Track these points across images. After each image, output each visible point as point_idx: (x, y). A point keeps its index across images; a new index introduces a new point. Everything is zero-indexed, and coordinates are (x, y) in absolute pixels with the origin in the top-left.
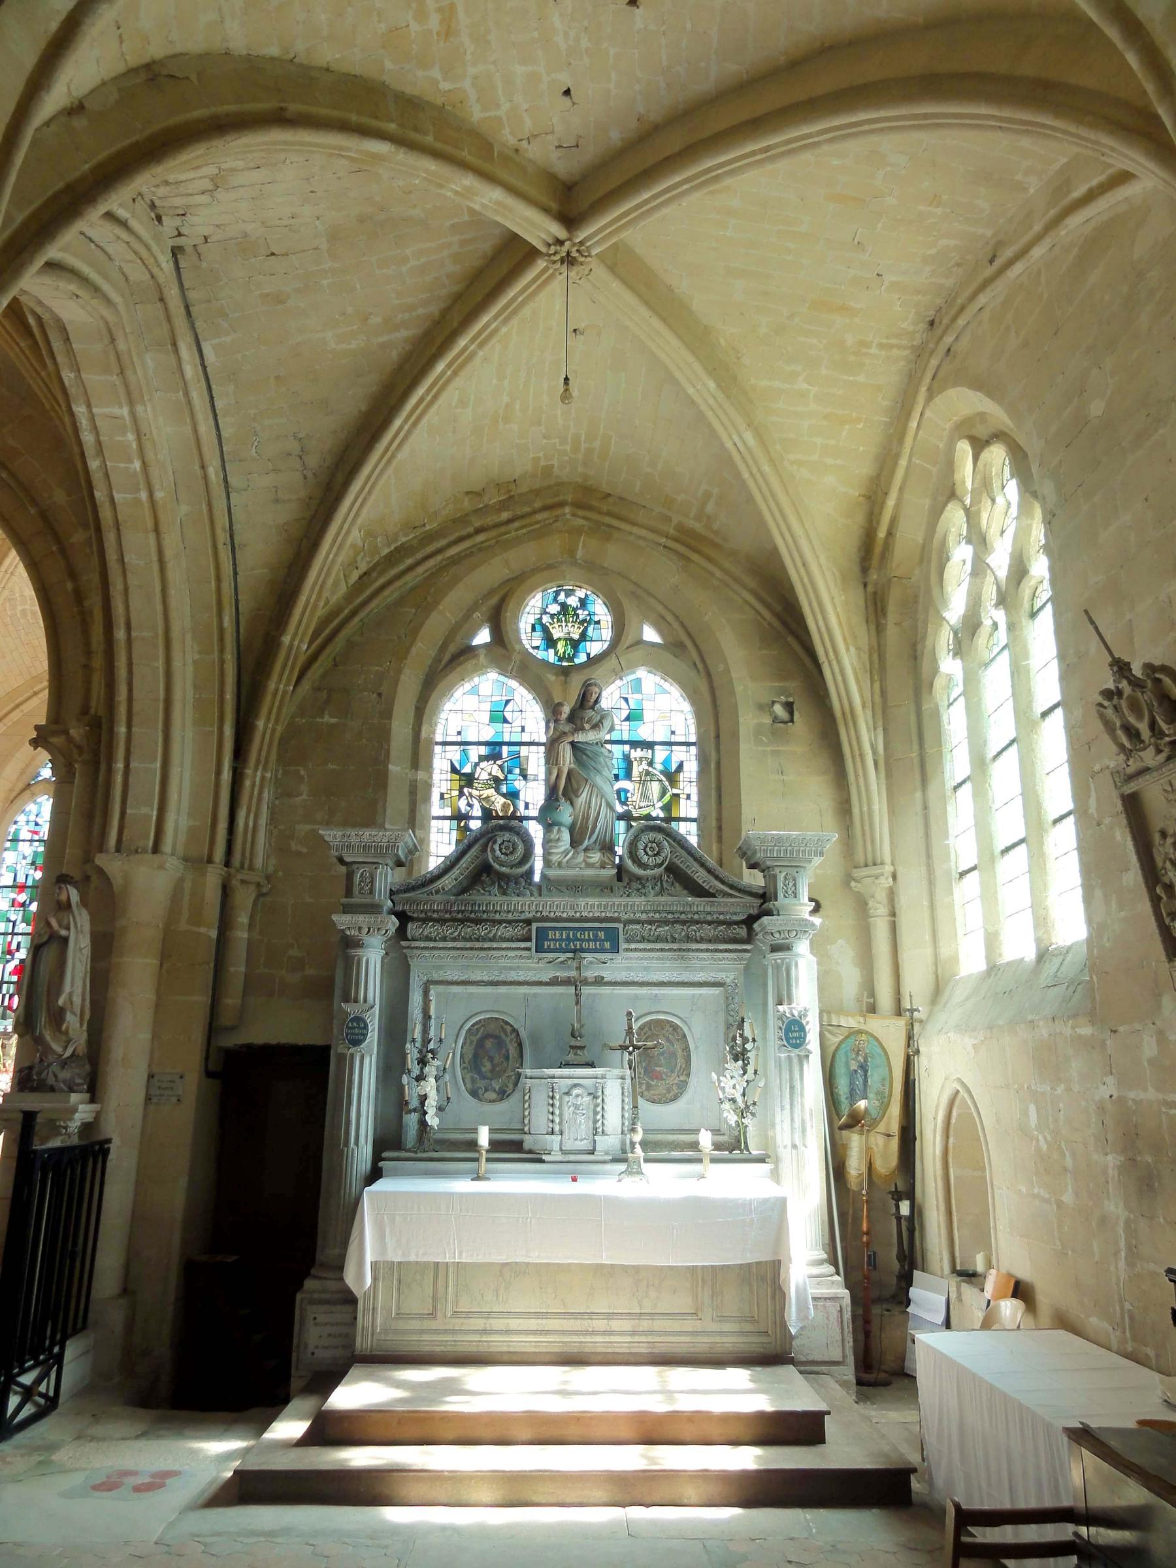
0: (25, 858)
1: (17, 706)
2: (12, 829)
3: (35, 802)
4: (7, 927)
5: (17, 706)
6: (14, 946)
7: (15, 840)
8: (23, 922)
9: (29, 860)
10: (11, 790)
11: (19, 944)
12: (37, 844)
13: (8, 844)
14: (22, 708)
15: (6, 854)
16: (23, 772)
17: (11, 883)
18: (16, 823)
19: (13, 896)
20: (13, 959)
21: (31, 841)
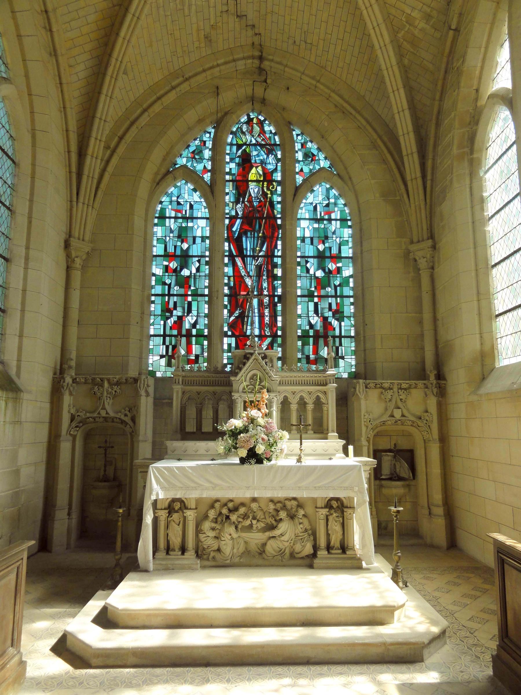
0: (172, 231)
1: (159, 98)
2: (159, 207)
3: (176, 187)
4: (163, 290)
5: (159, 98)
6: (171, 305)
7: (162, 217)
8: (176, 284)
9: (176, 233)
10: (157, 174)
11: (175, 303)
12: (180, 220)
13: (156, 221)
14: (163, 99)
15: (155, 229)
16: (164, 160)
17: (162, 252)
18: (161, 203)
19: (166, 263)
20: (172, 316)
21: (176, 218)
